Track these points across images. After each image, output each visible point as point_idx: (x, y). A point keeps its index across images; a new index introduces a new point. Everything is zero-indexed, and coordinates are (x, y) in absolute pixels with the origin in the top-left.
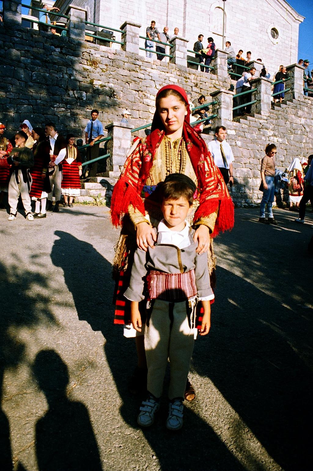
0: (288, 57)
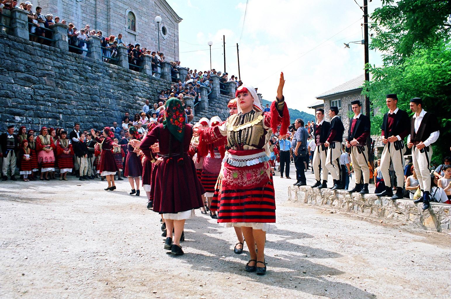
0: (173, 48)
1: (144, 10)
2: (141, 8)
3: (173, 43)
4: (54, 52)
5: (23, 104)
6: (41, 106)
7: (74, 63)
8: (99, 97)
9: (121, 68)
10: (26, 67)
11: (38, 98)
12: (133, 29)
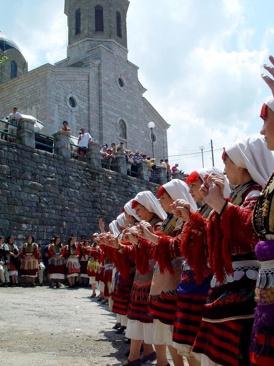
0: (162, 155)
1: (134, 118)
2: (132, 117)
3: (162, 149)
4: (58, 159)
5: (29, 212)
6: (46, 214)
7: (76, 169)
8: (100, 204)
9: (119, 174)
10: (33, 175)
11: (43, 205)
12: (124, 136)
